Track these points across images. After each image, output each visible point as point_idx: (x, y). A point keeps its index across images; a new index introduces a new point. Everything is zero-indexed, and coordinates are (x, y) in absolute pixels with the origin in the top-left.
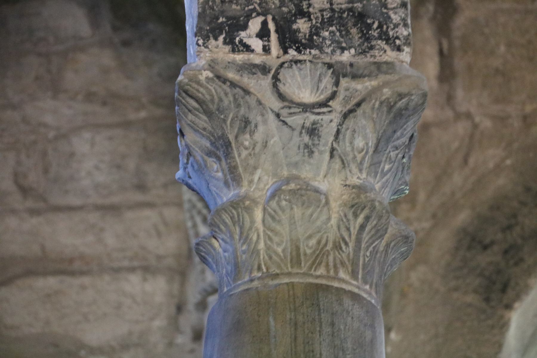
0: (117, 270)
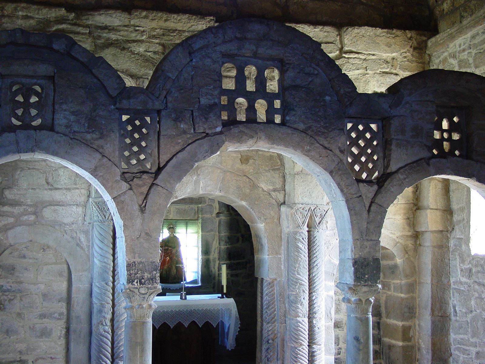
0: (70, 205)
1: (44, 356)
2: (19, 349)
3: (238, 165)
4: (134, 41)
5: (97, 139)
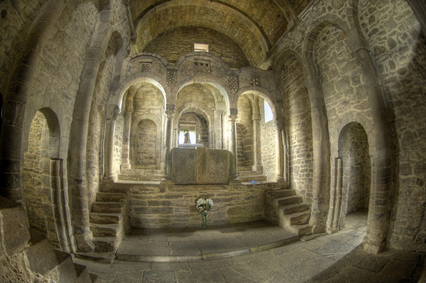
3: (202, 101)
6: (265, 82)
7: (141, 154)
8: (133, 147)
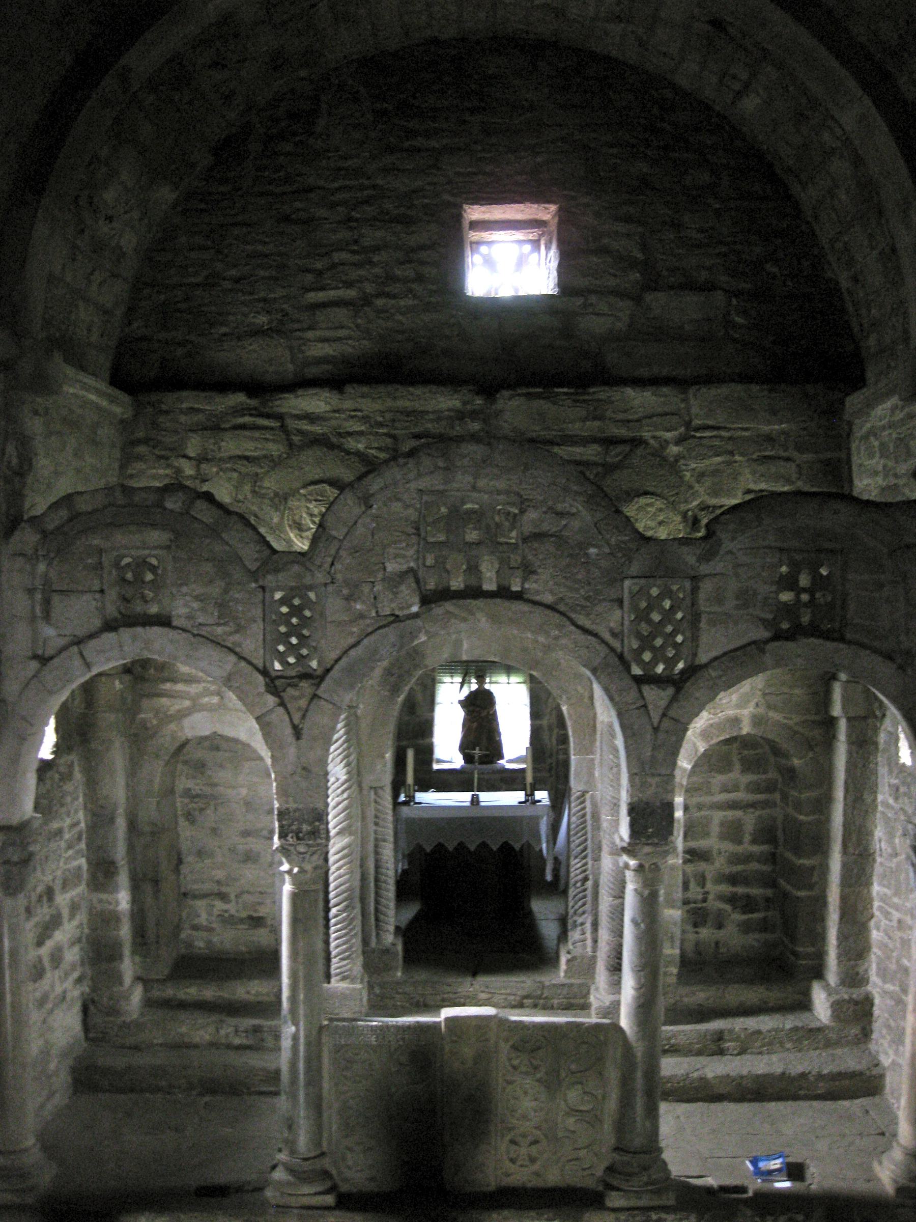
1: (251, 890)
2: (216, 878)
4: (350, 434)
5: (231, 634)
6: (881, 586)
7: (200, 905)
8: (148, 888)
